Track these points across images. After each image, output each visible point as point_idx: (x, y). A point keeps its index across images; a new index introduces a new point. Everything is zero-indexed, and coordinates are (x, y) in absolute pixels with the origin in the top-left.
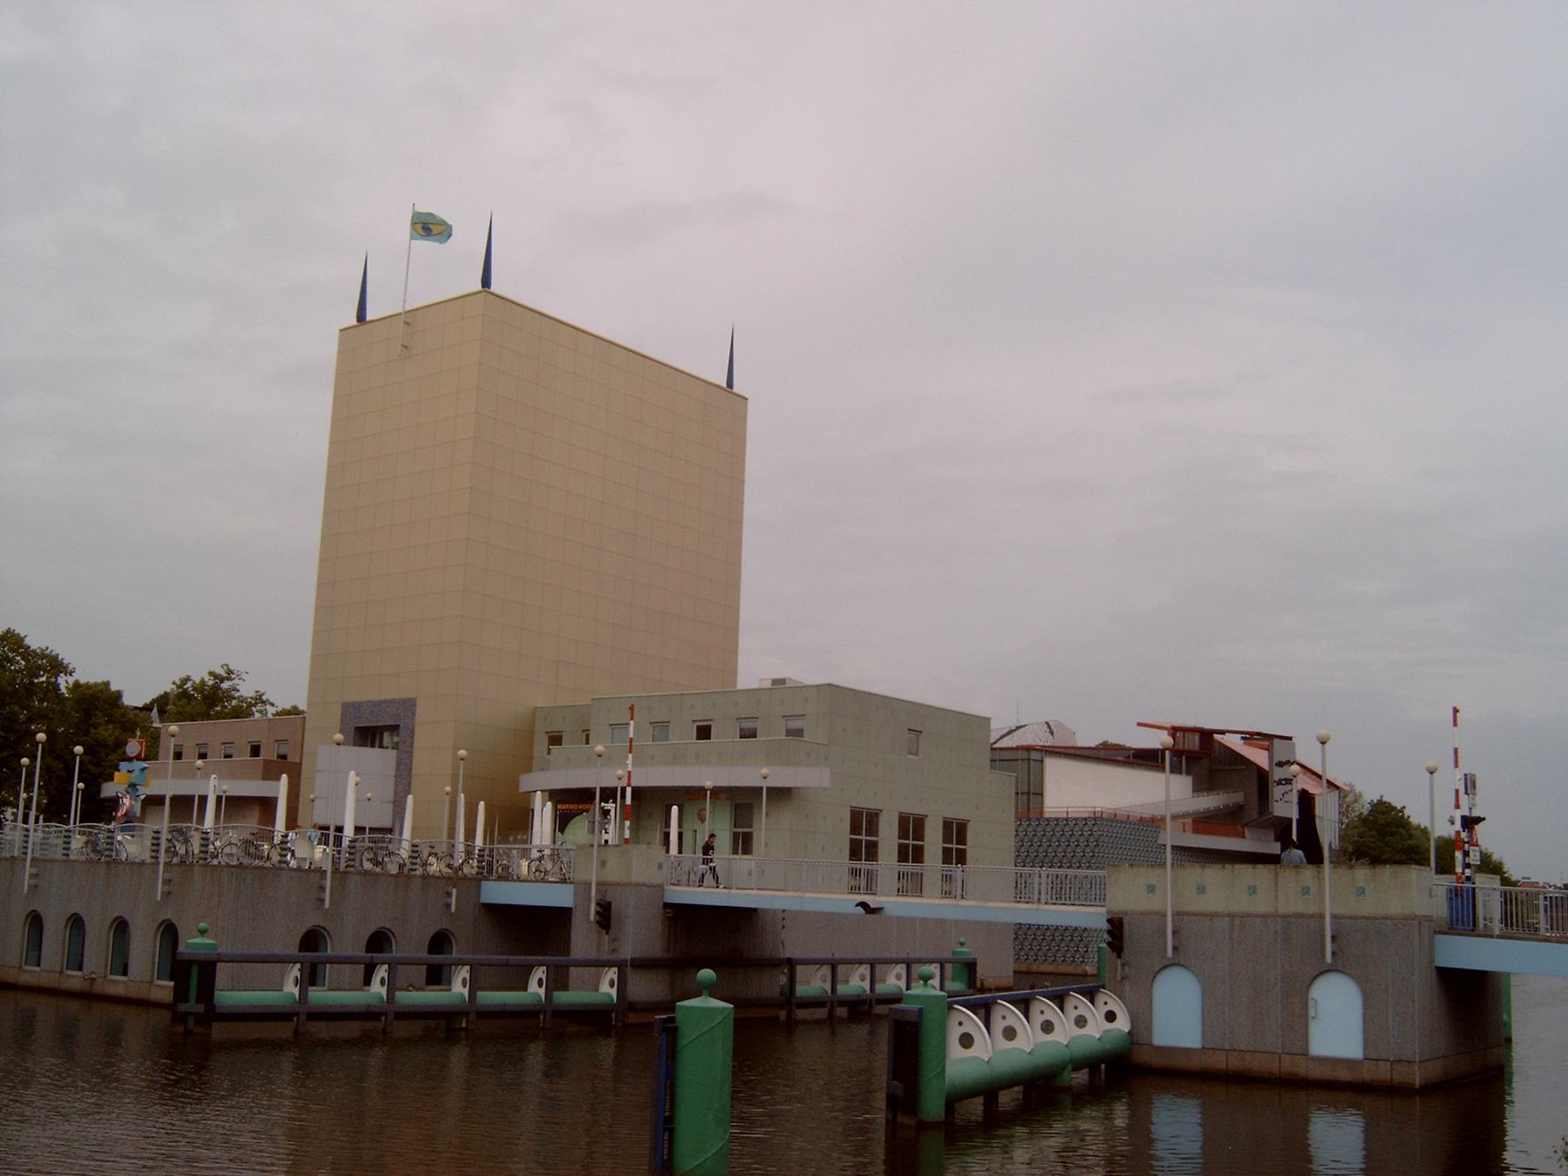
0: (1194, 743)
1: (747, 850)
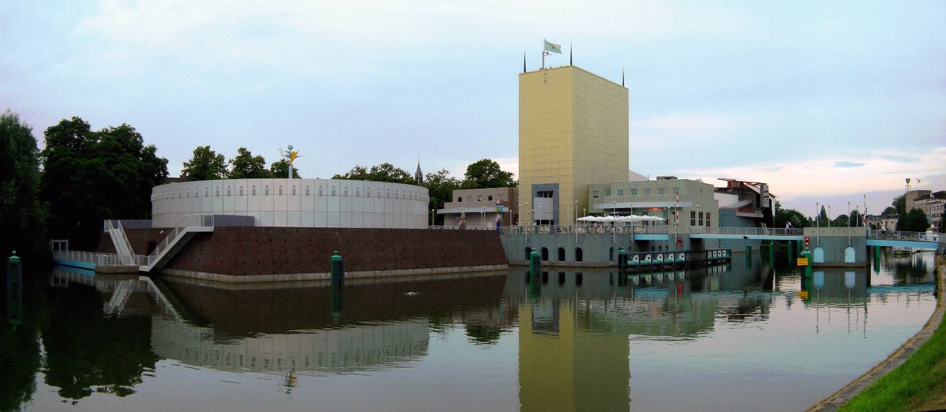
0: (738, 185)
1: (694, 225)
